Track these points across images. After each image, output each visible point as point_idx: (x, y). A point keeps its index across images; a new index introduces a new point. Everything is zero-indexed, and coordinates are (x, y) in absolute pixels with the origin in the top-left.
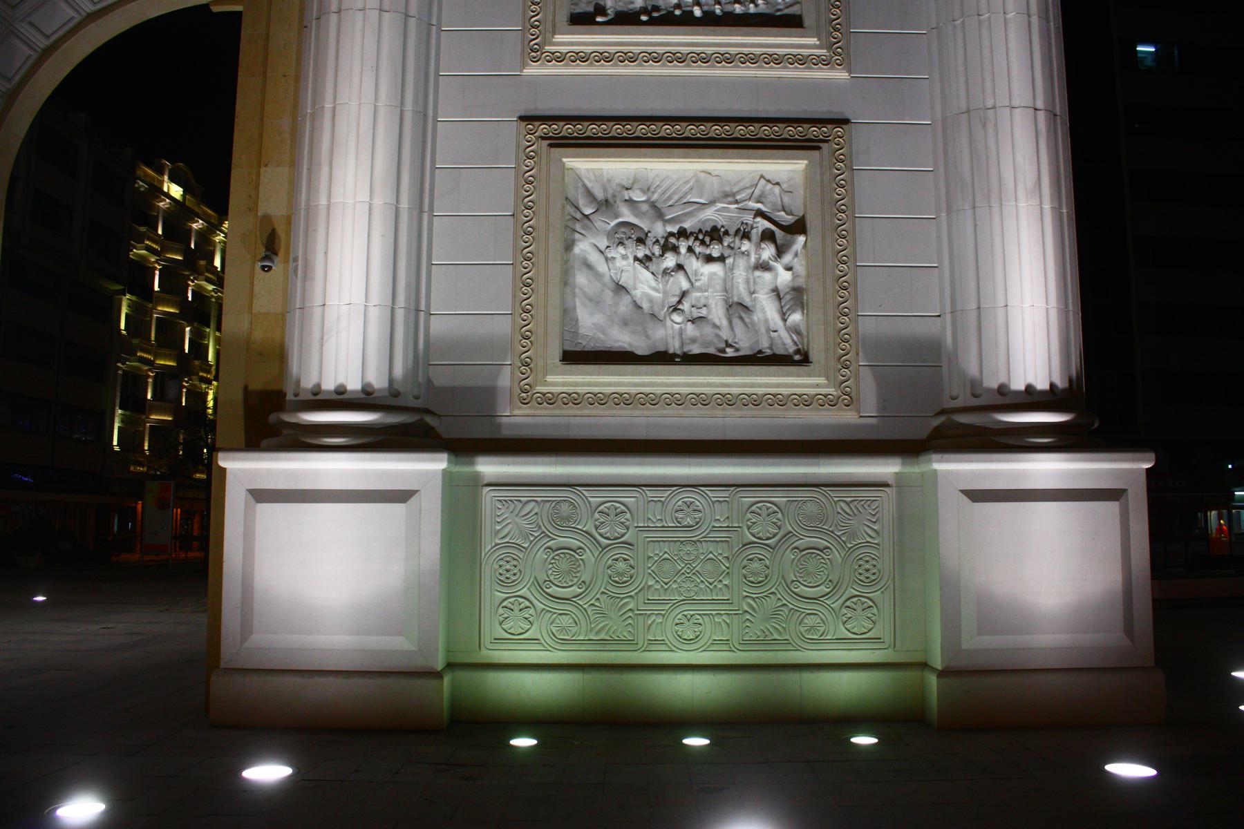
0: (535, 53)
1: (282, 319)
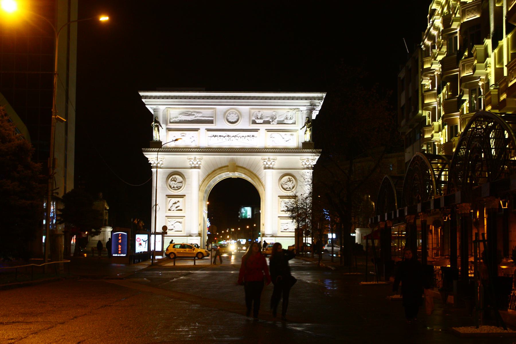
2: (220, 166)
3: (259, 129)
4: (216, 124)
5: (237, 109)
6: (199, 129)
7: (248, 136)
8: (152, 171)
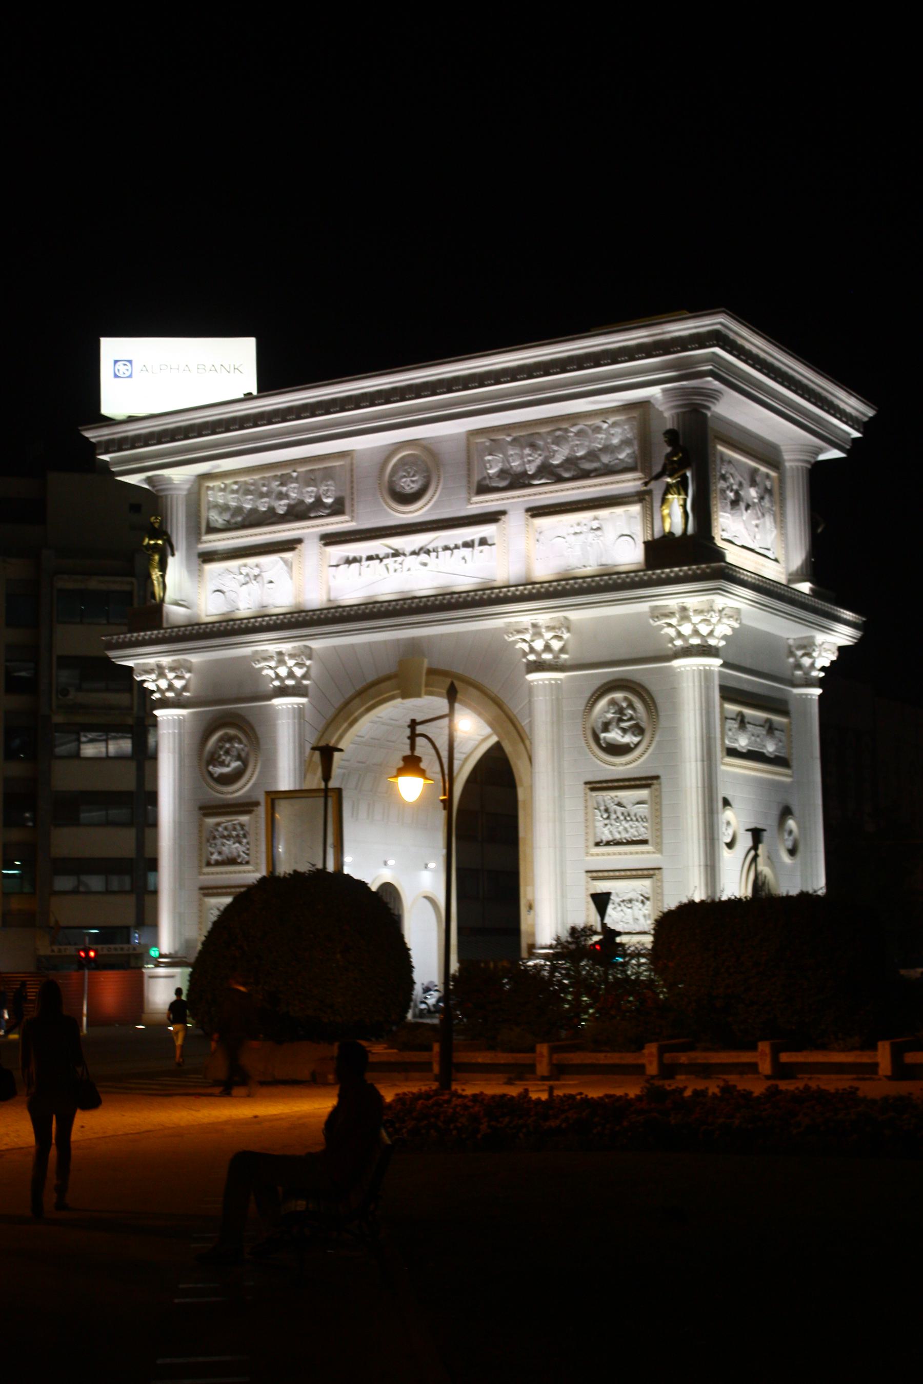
0: (587, 854)
1: (533, 926)
2: (371, 678)
3: (504, 513)
4: (353, 511)
5: (422, 442)
6: (299, 541)
7: (468, 545)
8: (156, 717)
